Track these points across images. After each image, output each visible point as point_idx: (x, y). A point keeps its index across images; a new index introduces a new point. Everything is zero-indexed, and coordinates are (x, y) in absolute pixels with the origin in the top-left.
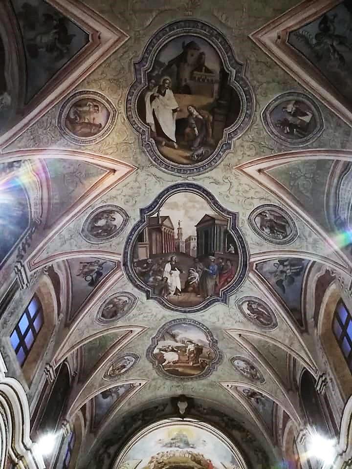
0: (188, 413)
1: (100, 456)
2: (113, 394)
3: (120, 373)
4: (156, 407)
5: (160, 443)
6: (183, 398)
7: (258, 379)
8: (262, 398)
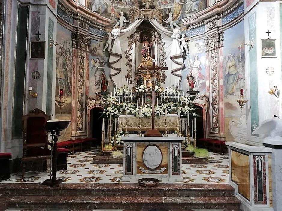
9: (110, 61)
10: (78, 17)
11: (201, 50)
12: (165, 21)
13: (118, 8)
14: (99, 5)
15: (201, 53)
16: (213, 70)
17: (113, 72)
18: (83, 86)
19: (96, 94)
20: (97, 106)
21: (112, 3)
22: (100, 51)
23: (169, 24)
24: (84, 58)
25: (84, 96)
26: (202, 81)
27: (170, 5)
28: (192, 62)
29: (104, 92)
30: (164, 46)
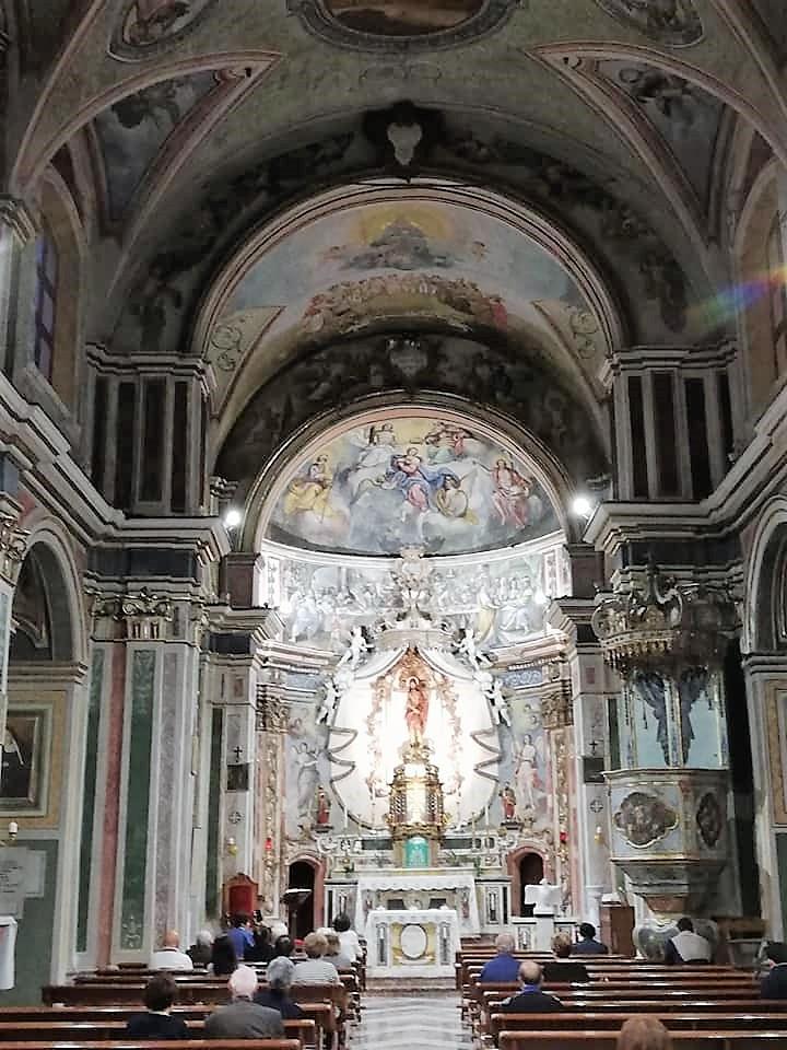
0: (425, 162)
1: (150, 299)
2: (157, 111)
3: (167, 33)
4: (315, 147)
5: (335, 257)
6: (404, 112)
7: (678, 27)
8: (686, 97)
9: (330, 747)
10: (268, 664)
11: (535, 722)
12: (458, 646)
13: (349, 616)
14: (307, 620)
15: (537, 729)
16: (558, 772)
17: (336, 770)
18: (275, 810)
19: (301, 827)
20: (303, 857)
21: (334, 607)
22: (310, 726)
23: (467, 652)
24: (277, 747)
25: (278, 835)
26: (540, 795)
27: (469, 606)
28: (519, 749)
29: (321, 823)
30: (455, 704)
